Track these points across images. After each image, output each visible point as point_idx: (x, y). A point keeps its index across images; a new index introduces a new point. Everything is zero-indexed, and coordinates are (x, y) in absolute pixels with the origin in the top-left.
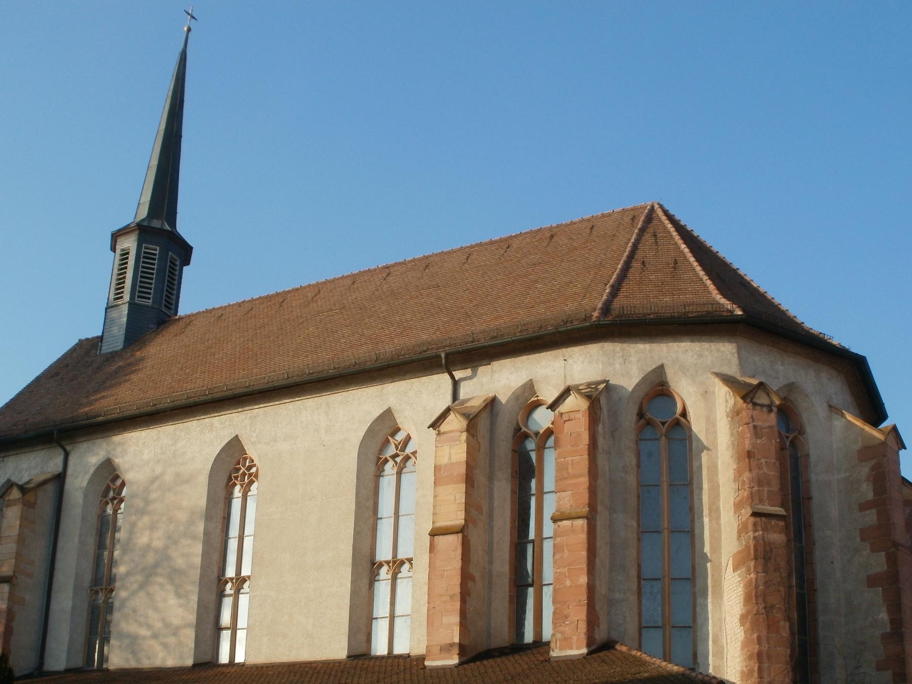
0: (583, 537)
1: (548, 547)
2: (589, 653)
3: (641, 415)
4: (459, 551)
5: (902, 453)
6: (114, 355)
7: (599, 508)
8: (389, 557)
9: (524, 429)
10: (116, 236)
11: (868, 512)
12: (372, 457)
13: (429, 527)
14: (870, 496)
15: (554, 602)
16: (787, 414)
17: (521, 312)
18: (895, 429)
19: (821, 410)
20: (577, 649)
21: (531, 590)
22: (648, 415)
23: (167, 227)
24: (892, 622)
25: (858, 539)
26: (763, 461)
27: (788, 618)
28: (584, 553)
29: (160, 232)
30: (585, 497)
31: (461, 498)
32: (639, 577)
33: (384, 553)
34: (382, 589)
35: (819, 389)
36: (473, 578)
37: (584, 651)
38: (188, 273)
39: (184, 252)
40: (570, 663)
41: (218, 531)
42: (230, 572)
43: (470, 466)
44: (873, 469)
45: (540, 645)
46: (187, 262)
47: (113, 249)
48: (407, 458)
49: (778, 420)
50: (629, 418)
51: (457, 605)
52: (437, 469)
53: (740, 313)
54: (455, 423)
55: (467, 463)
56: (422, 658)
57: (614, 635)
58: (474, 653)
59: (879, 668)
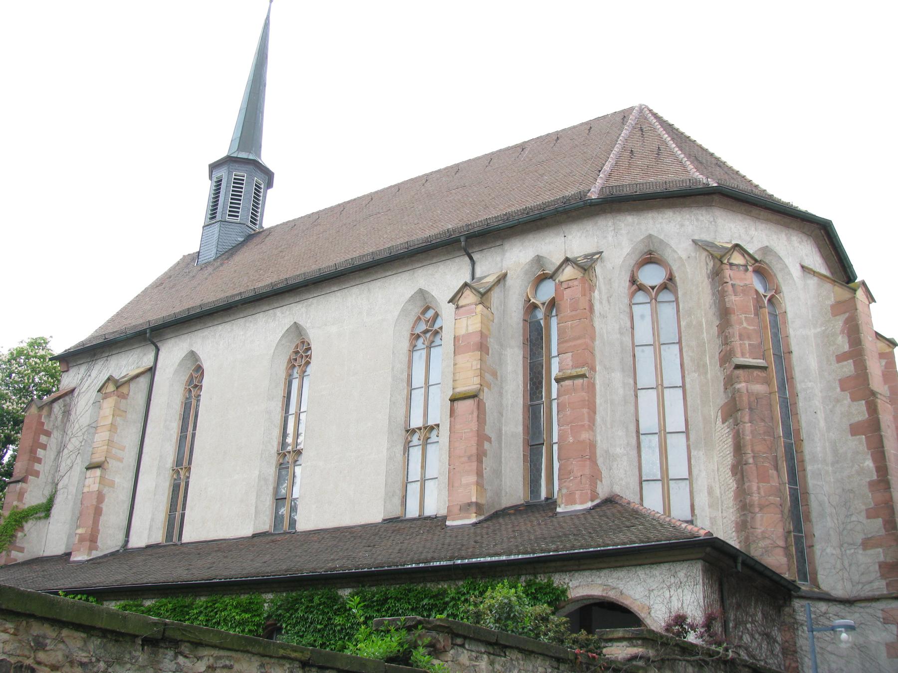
5: (872, 305)
6: (207, 264)
9: (533, 300)
11: (845, 363)
12: (406, 335)
14: (846, 348)
20: (582, 503)
25: (838, 389)
32: (638, 432)
36: (489, 440)
39: (269, 176)
41: (279, 409)
44: (846, 322)
48: (436, 333)
51: (474, 465)
56: (444, 518)
57: (617, 490)
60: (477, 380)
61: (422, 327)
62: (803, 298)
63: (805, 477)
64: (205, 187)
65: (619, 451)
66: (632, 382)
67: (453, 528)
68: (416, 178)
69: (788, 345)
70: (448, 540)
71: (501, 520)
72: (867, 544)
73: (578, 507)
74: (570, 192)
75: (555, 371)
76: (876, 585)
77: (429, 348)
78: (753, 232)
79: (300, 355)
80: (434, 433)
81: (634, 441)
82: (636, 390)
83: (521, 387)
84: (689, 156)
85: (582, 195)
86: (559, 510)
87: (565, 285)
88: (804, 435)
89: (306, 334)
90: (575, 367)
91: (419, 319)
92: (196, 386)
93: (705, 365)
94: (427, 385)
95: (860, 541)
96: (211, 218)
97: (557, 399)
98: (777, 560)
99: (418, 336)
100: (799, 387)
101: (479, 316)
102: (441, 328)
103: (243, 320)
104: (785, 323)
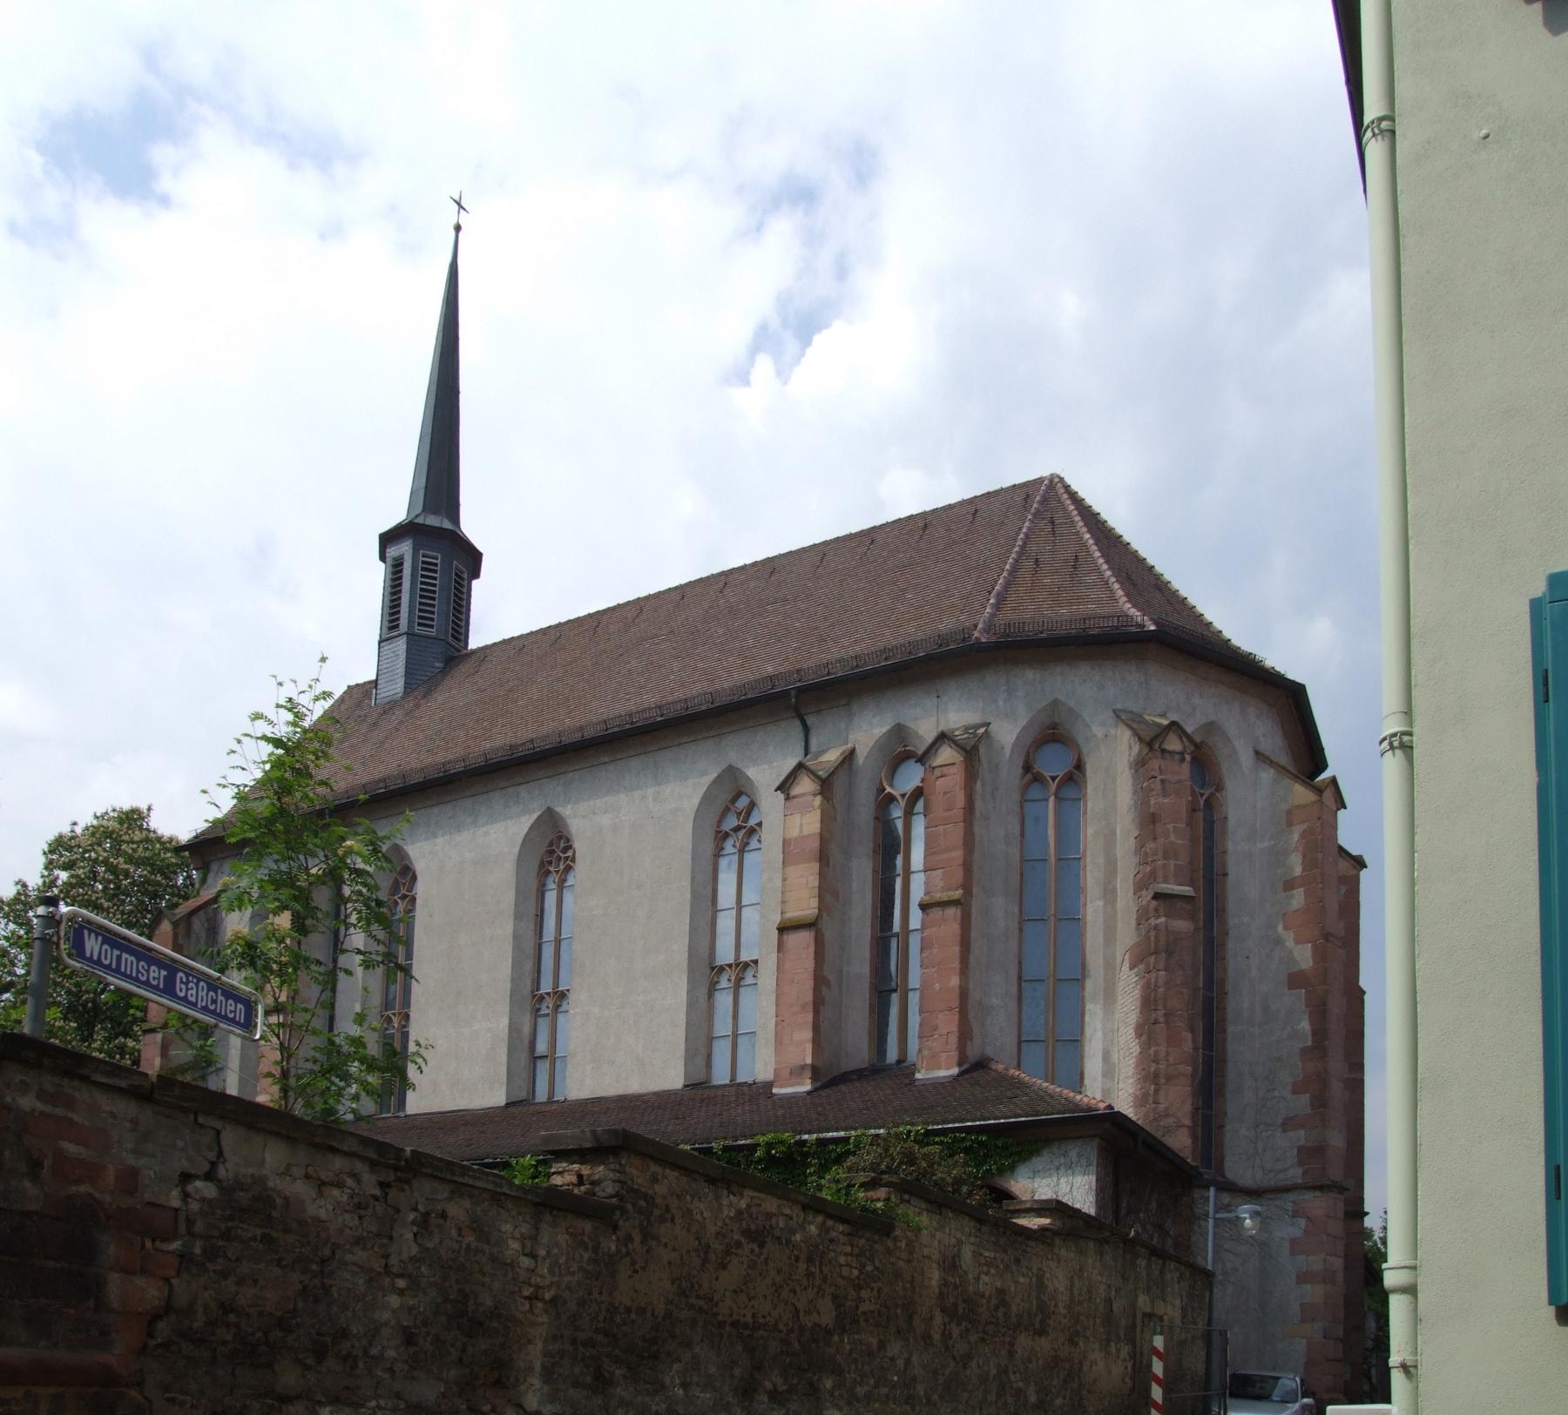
0: (955, 927)
1: (915, 943)
2: (961, 1074)
3: (1027, 768)
4: (812, 949)
5: (1341, 813)
7: (975, 890)
8: (730, 959)
10: (387, 539)
12: (710, 832)
13: (777, 919)
15: (921, 1012)
16: (1203, 762)
17: (887, 632)
18: (1334, 781)
19: (1246, 758)
20: (948, 1068)
21: (895, 997)
22: (1037, 768)
23: (447, 525)
24: (1314, 1033)
26: (1170, 826)
27: (1192, 1030)
28: (957, 949)
29: (440, 532)
30: (959, 876)
31: (814, 881)
32: (1020, 978)
33: (725, 955)
34: (724, 1000)
35: (1246, 732)
36: (828, 984)
37: (955, 1071)
38: (481, 591)
40: (938, 1085)
41: (531, 933)
42: (546, 987)
43: (825, 838)
45: (904, 1069)
46: (476, 574)
47: (383, 558)
48: (752, 831)
49: (1192, 777)
50: (1010, 774)
51: (810, 1017)
52: (786, 843)
53: (1153, 628)
54: (805, 785)
55: (821, 835)
56: (770, 1085)
57: (990, 1052)
58: (830, 1078)
59: (1297, 1089)
60: (815, 903)
61: (731, 822)
62: (1253, 795)
63: (1224, 1040)
64: (377, 573)
65: (995, 1001)
66: (1017, 910)
67: (783, 1098)
68: (708, 578)
69: (1224, 864)
70: (780, 1113)
71: (843, 1088)
72: (1288, 1124)
73: (943, 1073)
74: (946, 625)
75: (917, 892)
76: (1291, 1173)
77: (741, 852)
78: (1196, 701)
79: (551, 854)
80: (749, 974)
81: (1014, 989)
82: (1022, 922)
83: (869, 913)
84: (1117, 573)
85: (965, 634)
86: (918, 1076)
87: (937, 772)
88: (1229, 988)
89: (565, 825)
90: (943, 889)
91: (727, 810)
92: (404, 897)
93: (1114, 891)
94: (739, 906)
95: (1280, 1121)
96: (391, 628)
97: (922, 930)
98: (1180, 1142)
99: (727, 835)
100: (1232, 922)
101: (818, 812)
102: (760, 824)
103: (470, 801)
104: (1224, 832)
